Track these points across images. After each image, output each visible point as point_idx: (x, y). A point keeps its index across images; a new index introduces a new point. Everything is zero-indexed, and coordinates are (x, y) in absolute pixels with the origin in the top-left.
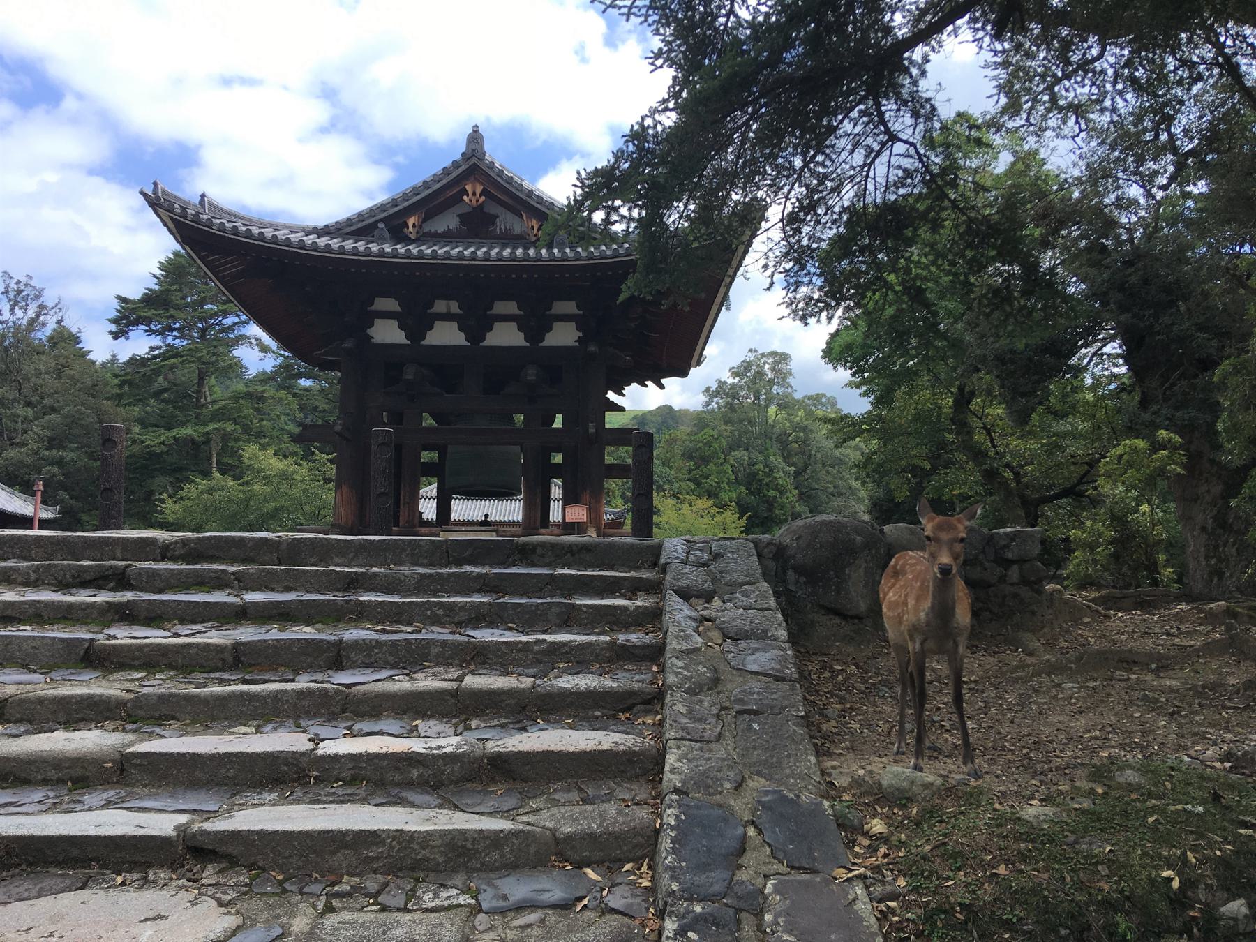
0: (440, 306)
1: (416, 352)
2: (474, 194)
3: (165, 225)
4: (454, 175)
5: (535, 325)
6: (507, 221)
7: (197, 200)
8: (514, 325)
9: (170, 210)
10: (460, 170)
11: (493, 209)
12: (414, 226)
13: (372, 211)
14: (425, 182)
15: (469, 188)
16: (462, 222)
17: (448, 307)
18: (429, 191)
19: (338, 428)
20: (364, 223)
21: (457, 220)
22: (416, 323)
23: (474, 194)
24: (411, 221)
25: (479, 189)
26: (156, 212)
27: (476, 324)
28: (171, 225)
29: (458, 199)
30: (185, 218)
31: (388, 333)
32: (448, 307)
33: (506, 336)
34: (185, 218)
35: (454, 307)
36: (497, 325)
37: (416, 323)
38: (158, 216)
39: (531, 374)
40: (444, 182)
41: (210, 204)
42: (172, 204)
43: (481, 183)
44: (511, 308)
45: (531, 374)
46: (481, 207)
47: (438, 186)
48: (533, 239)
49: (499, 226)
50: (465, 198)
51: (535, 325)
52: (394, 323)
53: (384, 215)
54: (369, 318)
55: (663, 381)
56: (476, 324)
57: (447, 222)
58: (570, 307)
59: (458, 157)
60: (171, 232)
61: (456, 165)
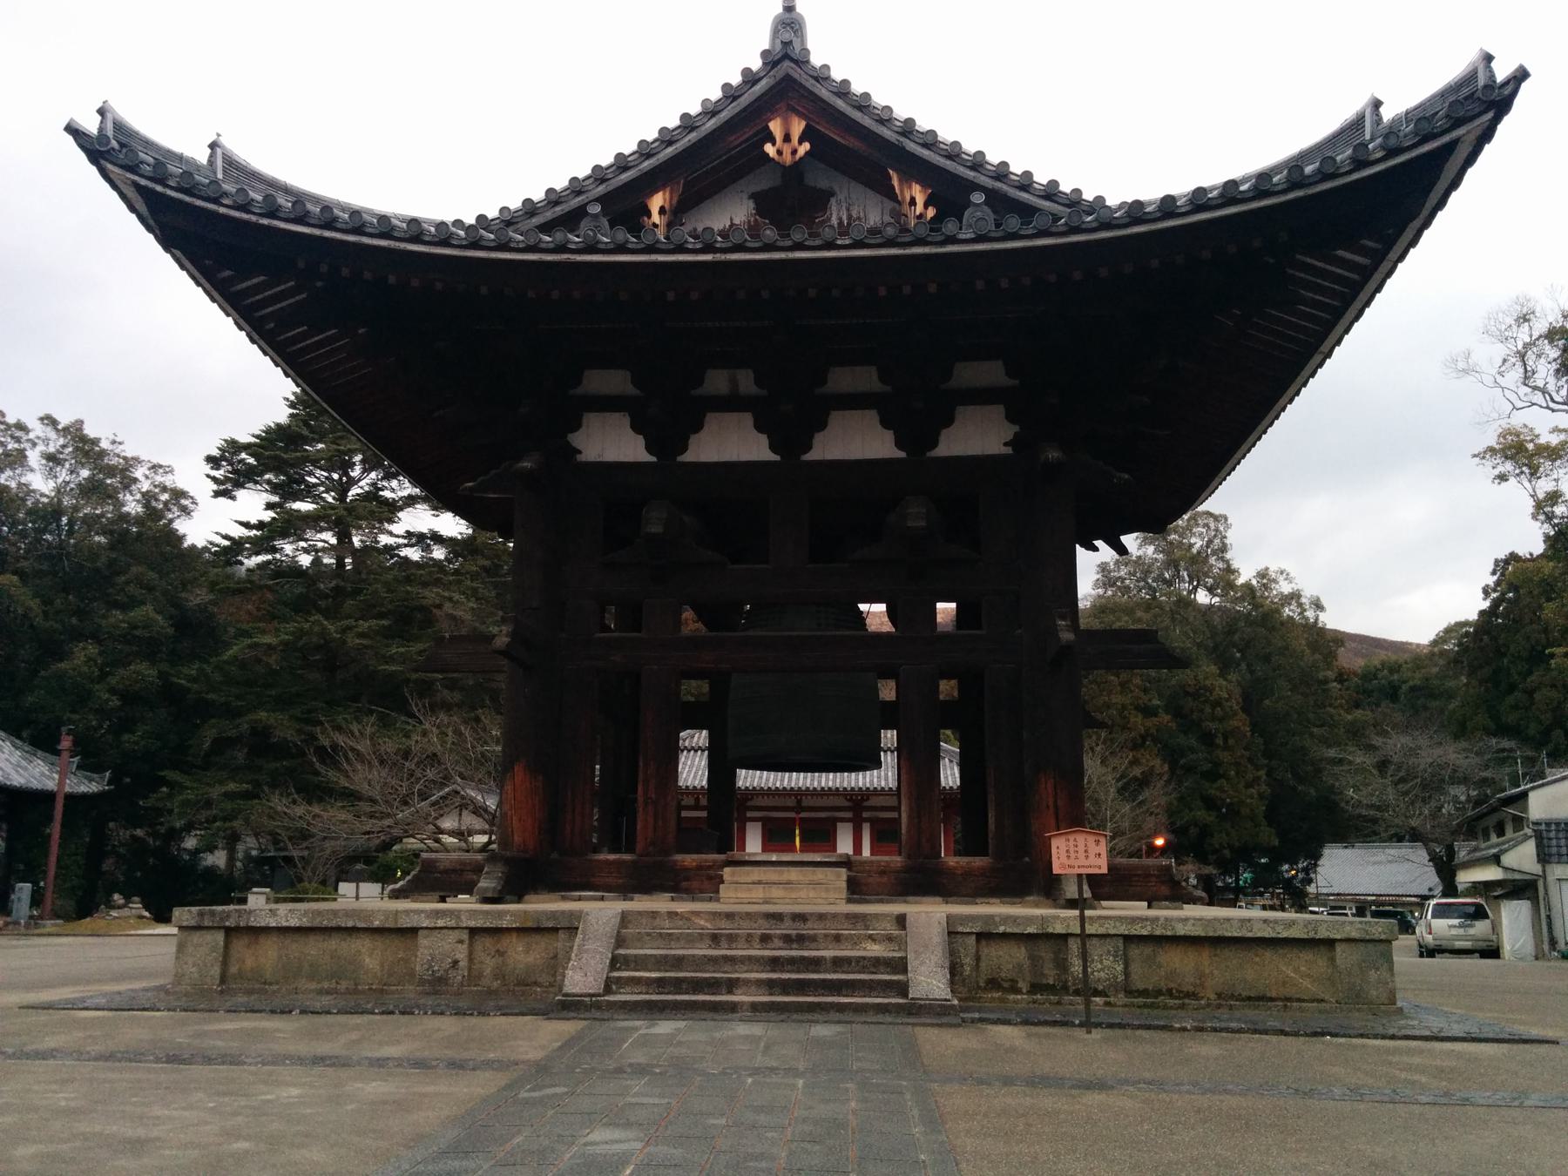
0: (717, 382)
1: (668, 474)
2: (787, 138)
3: (132, 208)
7: (202, 156)
8: (872, 416)
11: (820, 179)
12: (662, 211)
13: (576, 187)
15: (775, 127)
16: (760, 211)
17: (734, 382)
21: (751, 204)
23: (787, 138)
24: (657, 202)
25: (798, 127)
27: (791, 418)
30: (162, 181)
32: (734, 382)
33: (857, 440)
35: (747, 382)
36: (837, 419)
38: (114, 186)
39: (916, 515)
43: (801, 115)
45: (916, 515)
47: (712, 124)
49: (836, 214)
50: (769, 149)
53: (601, 189)
56: (791, 418)
58: (991, 373)
59: (756, 64)
61: (750, 78)
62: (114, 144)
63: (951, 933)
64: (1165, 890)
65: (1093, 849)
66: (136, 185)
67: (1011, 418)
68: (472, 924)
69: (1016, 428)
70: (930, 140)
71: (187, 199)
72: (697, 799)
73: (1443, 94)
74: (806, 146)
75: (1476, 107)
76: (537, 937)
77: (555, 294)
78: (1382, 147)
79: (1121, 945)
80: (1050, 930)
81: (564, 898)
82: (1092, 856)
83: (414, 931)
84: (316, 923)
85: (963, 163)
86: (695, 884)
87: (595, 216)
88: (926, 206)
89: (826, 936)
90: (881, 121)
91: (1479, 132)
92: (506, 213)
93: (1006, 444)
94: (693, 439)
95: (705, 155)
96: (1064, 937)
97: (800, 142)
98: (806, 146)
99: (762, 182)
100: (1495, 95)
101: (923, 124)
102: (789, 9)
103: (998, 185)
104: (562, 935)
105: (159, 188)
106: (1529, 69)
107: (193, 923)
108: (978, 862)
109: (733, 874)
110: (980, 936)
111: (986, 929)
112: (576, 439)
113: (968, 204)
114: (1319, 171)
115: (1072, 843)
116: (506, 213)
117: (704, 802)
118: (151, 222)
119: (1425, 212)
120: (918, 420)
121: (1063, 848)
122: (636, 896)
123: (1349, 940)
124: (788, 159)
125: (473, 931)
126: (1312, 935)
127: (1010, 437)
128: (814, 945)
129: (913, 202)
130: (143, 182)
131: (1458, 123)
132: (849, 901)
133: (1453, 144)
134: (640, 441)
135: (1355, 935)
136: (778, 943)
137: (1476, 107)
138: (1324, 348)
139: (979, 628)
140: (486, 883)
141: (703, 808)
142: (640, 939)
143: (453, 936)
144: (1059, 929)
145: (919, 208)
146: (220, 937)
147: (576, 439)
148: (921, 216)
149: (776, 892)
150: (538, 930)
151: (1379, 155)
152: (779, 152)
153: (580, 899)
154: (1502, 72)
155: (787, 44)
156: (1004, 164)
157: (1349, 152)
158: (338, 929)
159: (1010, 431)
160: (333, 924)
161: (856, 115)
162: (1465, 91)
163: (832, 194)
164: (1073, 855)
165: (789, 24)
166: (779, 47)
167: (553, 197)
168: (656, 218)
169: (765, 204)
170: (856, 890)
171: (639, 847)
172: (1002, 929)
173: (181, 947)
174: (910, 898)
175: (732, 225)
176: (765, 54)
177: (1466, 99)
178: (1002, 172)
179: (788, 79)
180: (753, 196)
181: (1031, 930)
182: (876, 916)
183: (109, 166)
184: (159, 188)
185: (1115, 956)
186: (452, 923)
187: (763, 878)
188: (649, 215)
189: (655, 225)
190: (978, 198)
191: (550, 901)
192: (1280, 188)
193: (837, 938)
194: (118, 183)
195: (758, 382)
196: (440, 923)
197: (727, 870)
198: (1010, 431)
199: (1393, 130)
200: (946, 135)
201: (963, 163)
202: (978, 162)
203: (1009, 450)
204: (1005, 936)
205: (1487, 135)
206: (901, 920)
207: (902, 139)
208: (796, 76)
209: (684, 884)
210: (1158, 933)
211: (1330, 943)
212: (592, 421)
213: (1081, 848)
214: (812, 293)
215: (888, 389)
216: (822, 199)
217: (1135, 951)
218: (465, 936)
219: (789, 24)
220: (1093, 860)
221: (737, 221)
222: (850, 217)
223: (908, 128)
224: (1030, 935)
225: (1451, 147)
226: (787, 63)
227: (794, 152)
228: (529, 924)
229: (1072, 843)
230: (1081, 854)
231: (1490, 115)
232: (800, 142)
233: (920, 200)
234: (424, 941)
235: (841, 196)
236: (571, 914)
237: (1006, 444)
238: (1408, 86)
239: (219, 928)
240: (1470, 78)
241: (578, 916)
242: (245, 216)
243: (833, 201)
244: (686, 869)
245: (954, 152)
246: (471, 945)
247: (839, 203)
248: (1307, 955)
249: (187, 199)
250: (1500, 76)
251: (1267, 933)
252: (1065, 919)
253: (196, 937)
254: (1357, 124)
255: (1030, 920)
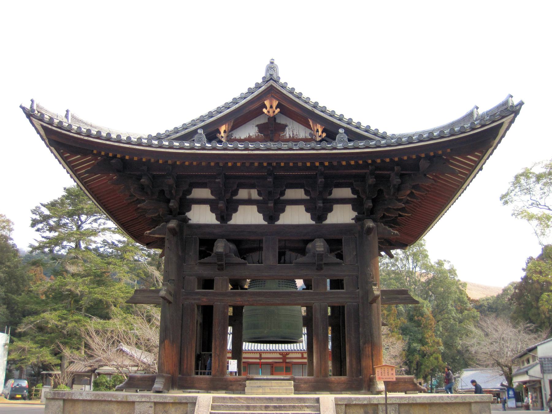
0: (243, 194)
2: (271, 107)
3: (38, 133)
4: (256, 93)
5: (319, 208)
6: (295, 130)
8: (302, 208)
9: (41, 119)
10: (261, 90)
11: (283, 120)
12: (225, 132)
14: (234, 99)
15: (267, 103)
17: (250, 194)
18: (237, 106)
19: (163, 293)
20: (187, 131)
21: (257, 129)
22: (225, 207)
23: (271, 107)
24: (223, 128)
26: (31, 122)
27: (272, 208)
28: (42, 132)
29: (258, 112)
30: (51, 124)
31: (202, 216)
32: (250, 194)
33: (296, 216)
34: (51, 124)
36: (289, 208)
37: (225, 207)
40: (249, 98)
41: (73, 117)
42: (42, 115)
43: (277, 99)
44: (299, 194)
45: (320, 246)
46: (274, 118)
47: (244, 101)
48: (319, 139)
49: (288, 134)
50: (265, 110)
51: (319, 208)
52: (207, 208)
53: (203, 124)
54: (186, 205)
55: (393, 252)
56: (272, 208)
57: (250, 131)
59: (260, 81)
60: (43, 139)
61: (258, 86)
62: (36, 112)
63: (337, 405)
64: (411, 387)
65: (390, 372)
66: (42, 126)
67: (354, 209)
68: (156, 400)
69: (356, 214)
70: (323, 110)
71: (59, 130)
72: (302, 355)
73: (498, 107)
74: (278, 110)
75: (509, 112)
76: (179, 406)
77: (187, 163)
78: (479, 124)
79: (397, 407)
80: (372, 402)
81: (184, 392)
82: (390, 374)
83: (133, 403)
84: (97, 398)
85: (336, 118)
86: (234, 387)
87: (201, 134)
88: (322, 132)
89: (290, 406)
90: (306, 102)
91: (510, 120)
92: (168, 132)
93: (352, 219)
94: (234, 215)
95: (242, 113)
96: (377, 405)
97: (276, 108)
98: (278, 110)
99: (261, 120)
100: (514, 110)
101: (321, 104)
102: (272, 63)
103: (348, 126)
104: (189, 405)
105: (50, 127)
106: (524, 101)
107: (51, 397)
108: (343, 378)
109: (250, 383)
110: (346, 405)
111: (349, 402)
112: (189, 215)
113: (338, 133)
114: (459, 131)
115: (383, 370)
116: (168, 132)
117: (305, 355)
118: (45, 137)
119: (495, 145)
120: (319, 209)
121: (380, 372)
122: (212, 391)
123: (476, 402)
124: (271, 114)
125: (156, 403)
126: (464, 401)
127: (354, 216)
128: (285, 409)
129: (318, 131)
130: (45, 125)
131: (503, 117)
132: (295, 394)
133: (502, 124)
134: (214, 216)
135: (478, 400)
136: (273, 409)
137: (509, 112)
138: (464, 187)
139: (343, 289)
140: (158, 385)
141: (305, 358)
142: (219, 407)
143: (149, 404)
144: (375, 402)
145: (320, 133)
146: (61, 403)
147: (189, 215)
148: (320, 136)
149: (267, 390)
150: (180, 403)
151: (479, 126)
152: (268, 112)
153: (190, 392)
154: (516, 101)
155: (271, 75)
156: (351, 119)
157: (469, 125)
158: (105, 401)
159: (354, 214)
160: (104, 399)
161: (297, 100)
162: (505, 107)
163: (286, 126)
164: (383, 374)
165: (272, 66)
166: (268, 76)
167: (185, 127)
168: (222, 134)
169: (261, 128)
170: (297, 389)
171: (213, 372)
172: (354, 402)
173: (47, 406)
174: (317, 392)
175: (249, 136)
176: (264, 78)
177: (505, 109)
178: (349, 122)
179: (271, 86)
180: (257, 126)
181: (365, 402)
182: (308, 399)
183: (34, 119)
184: (50, 127)
185: (395, 411)
186: (148, 400)
187: (261, 385)
188: (220, 133)
189: (222, 137)
190: (341, 131)
191: (179, 393)
192: (447, 135)
193: (294, 407)
194: (36, 125)
195: (259, 194)
196: (143, 400)
197: (248, 382)
198: (354, 214)
199: (482, 118)
200: (330, 108)
201: (336, 118)
202: (341, 118)
203: (353, 222)
204: (355, 405)
205: (512, 121)
206: (318, 400)
207: (313, 109)
208: (275, 86)
209: (230, 387)
210: (410, 402)
211: (470, 404)
212: (195, 208)
213: (386, 372)
214: (282, 164)
215: (308, 198)
216: (283, 127)
217: (402, 409)
218: (153, 405)
219: (272, 66)
220: (390, 376)
221: (251, 135)
222: (293, 134)
223: (315, 105)
224: (365, 405)
225: (501, 125)
226: (271, 81)
227: (274, 112)
228: (177, 401)
229: (383, 370)
230: (386, 374)
231: (513, 115)
232: (276, 108)
233: (320, 130)
234: (137, 406)
235: (290, 127)
236: (193, 397)
237: (352, 219)
238: (486, 104)
239: (61, 399)
240: (506, 103)
241: (196, 398)
242: (79, 136)
243: (287, 128)
244: (231, 381)
245: (332, 114)
246: (155, 409)
247: (289, 129)
248: (462, 408)
249: (59, 130)
250: (515, 103)
251: (449, 401)
252: (378, 398)
253: (53, 402)
254: (471, 114)
255: (365, 399)
